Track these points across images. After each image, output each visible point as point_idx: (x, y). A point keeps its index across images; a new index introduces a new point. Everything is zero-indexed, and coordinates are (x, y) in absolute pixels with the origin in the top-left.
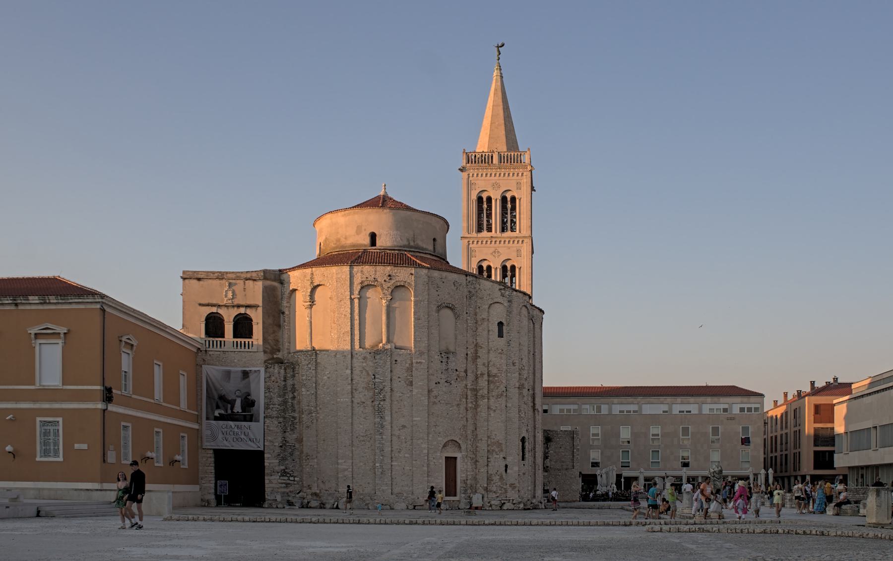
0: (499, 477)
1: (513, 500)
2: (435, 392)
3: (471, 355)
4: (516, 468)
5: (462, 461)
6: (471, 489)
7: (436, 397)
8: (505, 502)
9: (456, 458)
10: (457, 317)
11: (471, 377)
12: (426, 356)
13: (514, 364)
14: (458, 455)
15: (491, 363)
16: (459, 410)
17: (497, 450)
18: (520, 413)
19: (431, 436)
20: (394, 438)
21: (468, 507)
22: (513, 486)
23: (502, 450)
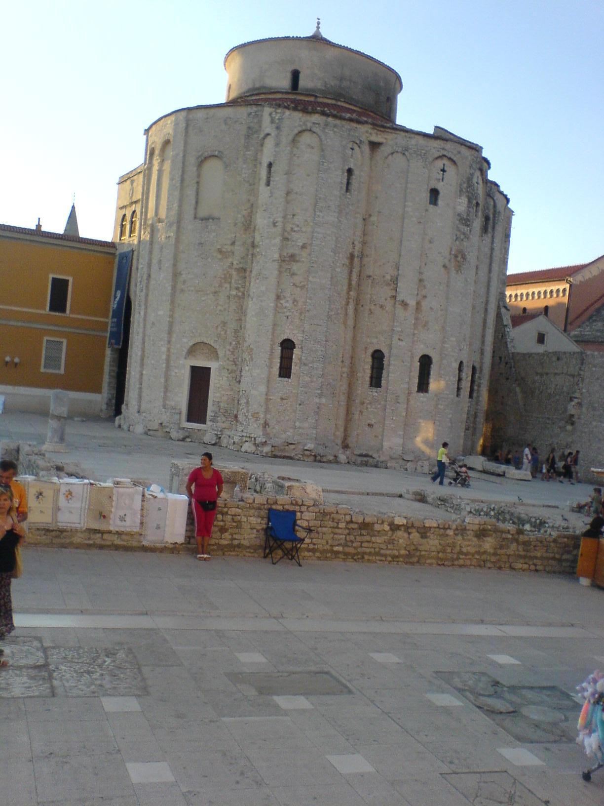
0: (245, 401)
1: (255, 438)
2: (183, 276)
3: (243, 220)
4: (263, 389)
5: (217, 374)
6: (224, 415)
7: (184, 282)
8: (247, 439)
9: (209, 369)
10: (226, 166)
11: (239, 250)
12: (174, 228)
13: (274, 224)
14: (213, 365)
15: (257, 227)
16: (217, 300)
17: (247, 359)
18: (281, 302)
19: (174, 336)
20: (146, 338)
21: (213, 442)
22: (256, 415)
23: (252, 359)
